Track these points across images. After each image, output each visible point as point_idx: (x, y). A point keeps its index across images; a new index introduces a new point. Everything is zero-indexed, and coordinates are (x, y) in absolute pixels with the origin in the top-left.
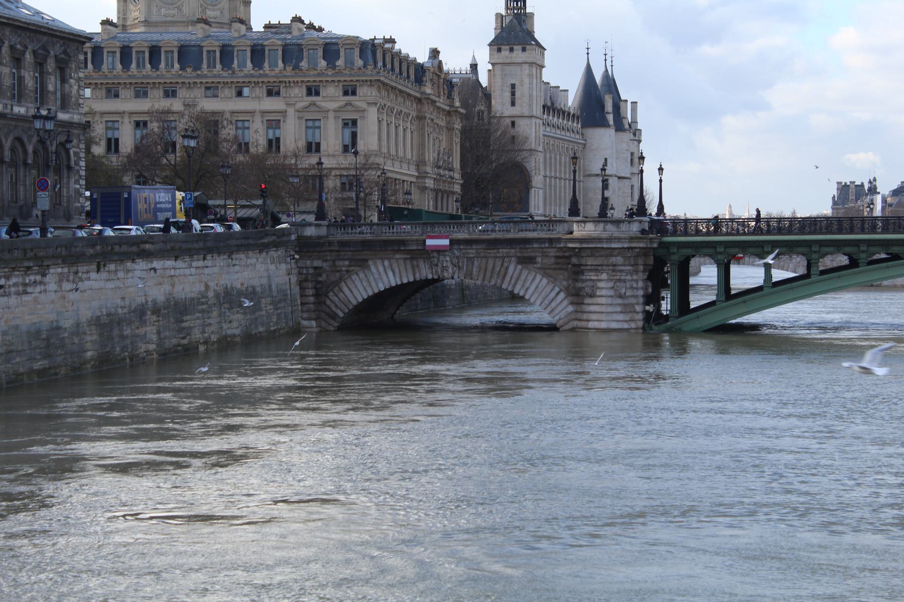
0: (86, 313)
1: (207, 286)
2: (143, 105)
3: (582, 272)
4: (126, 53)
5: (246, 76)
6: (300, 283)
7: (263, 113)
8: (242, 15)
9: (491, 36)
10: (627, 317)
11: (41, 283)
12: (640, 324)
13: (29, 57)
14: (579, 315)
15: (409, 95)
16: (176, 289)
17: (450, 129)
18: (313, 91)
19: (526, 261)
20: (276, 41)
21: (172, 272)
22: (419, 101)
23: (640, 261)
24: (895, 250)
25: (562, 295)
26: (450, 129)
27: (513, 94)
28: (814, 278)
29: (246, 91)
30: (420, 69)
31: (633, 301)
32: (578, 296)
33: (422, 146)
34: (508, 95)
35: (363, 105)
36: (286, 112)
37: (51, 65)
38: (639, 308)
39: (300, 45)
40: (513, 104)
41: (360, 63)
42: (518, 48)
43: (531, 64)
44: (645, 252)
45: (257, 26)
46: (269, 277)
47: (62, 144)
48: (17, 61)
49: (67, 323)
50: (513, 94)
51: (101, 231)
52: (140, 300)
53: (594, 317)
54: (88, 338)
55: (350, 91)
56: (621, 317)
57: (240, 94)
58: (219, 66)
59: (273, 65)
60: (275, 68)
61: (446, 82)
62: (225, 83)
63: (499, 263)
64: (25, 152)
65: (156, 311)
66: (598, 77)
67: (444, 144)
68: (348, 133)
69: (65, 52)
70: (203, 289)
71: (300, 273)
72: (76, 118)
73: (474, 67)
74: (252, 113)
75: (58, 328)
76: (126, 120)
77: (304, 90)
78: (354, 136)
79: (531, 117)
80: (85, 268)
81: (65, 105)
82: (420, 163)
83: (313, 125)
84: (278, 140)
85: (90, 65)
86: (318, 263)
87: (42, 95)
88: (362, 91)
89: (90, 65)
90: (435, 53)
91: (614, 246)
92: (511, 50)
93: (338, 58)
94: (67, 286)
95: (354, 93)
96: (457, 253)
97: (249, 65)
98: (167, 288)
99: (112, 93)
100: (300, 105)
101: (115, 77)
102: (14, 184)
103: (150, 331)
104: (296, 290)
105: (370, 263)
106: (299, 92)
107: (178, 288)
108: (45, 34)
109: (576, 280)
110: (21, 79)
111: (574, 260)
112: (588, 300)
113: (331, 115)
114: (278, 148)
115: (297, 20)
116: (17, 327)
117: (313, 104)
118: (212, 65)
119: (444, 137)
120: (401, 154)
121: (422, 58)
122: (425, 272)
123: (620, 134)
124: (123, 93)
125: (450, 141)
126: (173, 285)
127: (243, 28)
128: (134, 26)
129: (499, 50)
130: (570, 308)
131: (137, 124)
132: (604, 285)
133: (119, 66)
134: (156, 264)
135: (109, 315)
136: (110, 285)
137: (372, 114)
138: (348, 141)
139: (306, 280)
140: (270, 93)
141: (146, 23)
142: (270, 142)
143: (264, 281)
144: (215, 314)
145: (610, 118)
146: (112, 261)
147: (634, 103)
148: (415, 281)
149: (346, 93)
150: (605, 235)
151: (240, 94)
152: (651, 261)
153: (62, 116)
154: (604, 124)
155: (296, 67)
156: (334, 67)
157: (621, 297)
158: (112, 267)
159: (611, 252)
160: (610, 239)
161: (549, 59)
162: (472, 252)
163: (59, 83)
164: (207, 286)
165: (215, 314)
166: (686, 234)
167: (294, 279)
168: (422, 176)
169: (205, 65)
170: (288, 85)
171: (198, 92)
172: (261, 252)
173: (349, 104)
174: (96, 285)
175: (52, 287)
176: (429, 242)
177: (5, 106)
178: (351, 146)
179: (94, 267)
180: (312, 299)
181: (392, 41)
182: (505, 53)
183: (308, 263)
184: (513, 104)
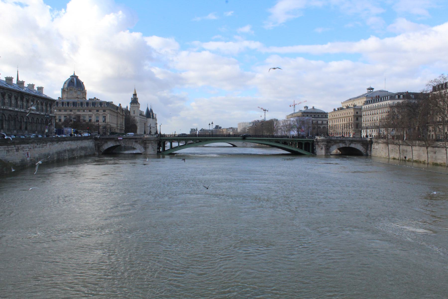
1: (77, 146)
2: (66, 113)
3: (146, 144)
4: (63, 103)
5: (85, 108)
6: (95, 146)
7: (88, 115)
8: (84, 97)
9: (130, 102)
10: (154, 152)
11: (46, 145)
12: (156, 153)
13: (44, 104)
14: (146, 151)
15: (115, 112)
16: (72, 147)
17: (123, 118)
18: (98, 111)
19: (136, 142)
20: (91, 102)
21: (71, 144)
22: (117, 113)
23: (157, 142)
24: (201, 140)
25: (143, 148)
26: (123, 118)
27: (134, 112)
28: (187, 145)
29: (85, 111)
30: (117, 107)
31: (155, 149)
32: (145, 148)
33: (118, 121)
34: (133, 112)
35: (107, 114)
36: (92, 115)
37: (48, 105)
38: (156, 150)
39: (95, 103)
40: (134, 114)
41: (106, 106)
42: (135, 104)
43: (137, 107)
44: (157, 140)
45: (87, 99)
46: (89, 145)
47: (50, 120)
48: (42, 104)
49: (51, 153)
50: (134, 112)
51: (58, 136)
52: (65, 149)
53: (148, 152)
54: (55, 156)
55: (104, 111)
56: (153, 152)
57: (84, 111)
58: (80, 106)
59: (90, 106)
60: (91, 107)
61: (122, 110)
62: (81, 109)
63: (131, 142)
64: (43, 121)
65: (68, 151)
66: (149, 110)
67: (122, 121)
68: (104, 118)
69: (51, 103)
70: (77, 146)
71: (95, 144)
72: (53, 115)
73: (127, 107)
74: (86, 115)
75: (49, 154)
76: (63, 116)
77: (96, 111)
78: (105, 119)
79: (137, 116)
80: (54, 143)
81: (51, 113)
82: (117, 124)
83: (97, 117)
84: (91, 120)
85: (56, 106)
86: (98, 142)
87: (47, 111)
89: (56, 106)
90: (120, 104)
91: (152, 139)
92: (134, 104)
93: (102, 105)
94: (51, 146)
95: (105, 111)
96: (124, 140)
97: (86, 106)
99: (60, 110)
100: (95, 113)
101: (61, 108)
102: (41, 127)
103: (67, 154)
104: (94, 147)
105: (108, 142)
106: (95, 111)
107: (72, 147)
108: (47, 100)
109: (145, 145)
110: (43, 108)
111: (145, 142)
112: (147, 149)
113: (101, 115)
114: (91, 121)
115: (95, 98)
116: (41, 154)
117: (98, 113)
118: (79, 106)
119: (122, 120)
120: (114, 122)
121: (118, 105)
122: (118, 144)
124: (62, 111)
125: (123, 120)
126: (71, 146)
127: (85, 99)
128: (64, 98)
129: (132, 104)
130: (144, 150)
131: (65, 116)
132: (150, 146)
133: (61, 106)
134: (68, 142)
135: (59, 151)
136: (59, 146)
137: (109, 115)
138: (104, 120)
139: (96, 145)
140: (90, 111)
141: (67, 98)
142: (90, 120)
143: (88, 145)
144: (79, 151)
145: (151, 117)
146: (60, 141)
147: (156, 114)
148: (116, 145)
149: (104, 111)
150: (150, 137)
151: (84, 111)
152: (158, 142)
153: (50, 115)
154: (150, 118)
155: (95, 106)
156: (102, 107)
157: (153, 148)
158: (60, 143)
159: (151, 140)
160: (151, 138)
161: (141, 106)
162: (126, 140)
164: (77, 146)
165: (79, 151)
166: (165, 137)
167: (94, 145)
168: (117, 126)
169: (78, 106)
170: (93, 110)
171: (76, 111)
172: (88, 140)
173: (104, 113)
174: (56, 146)
175: (48, 146)
176: (119, 138)
177: (40, 113)
178: (104, 121)
179: (56, 143)
180: (97, 149)
181: (112, 102)
183: (97, 142)
184: (134, 114)
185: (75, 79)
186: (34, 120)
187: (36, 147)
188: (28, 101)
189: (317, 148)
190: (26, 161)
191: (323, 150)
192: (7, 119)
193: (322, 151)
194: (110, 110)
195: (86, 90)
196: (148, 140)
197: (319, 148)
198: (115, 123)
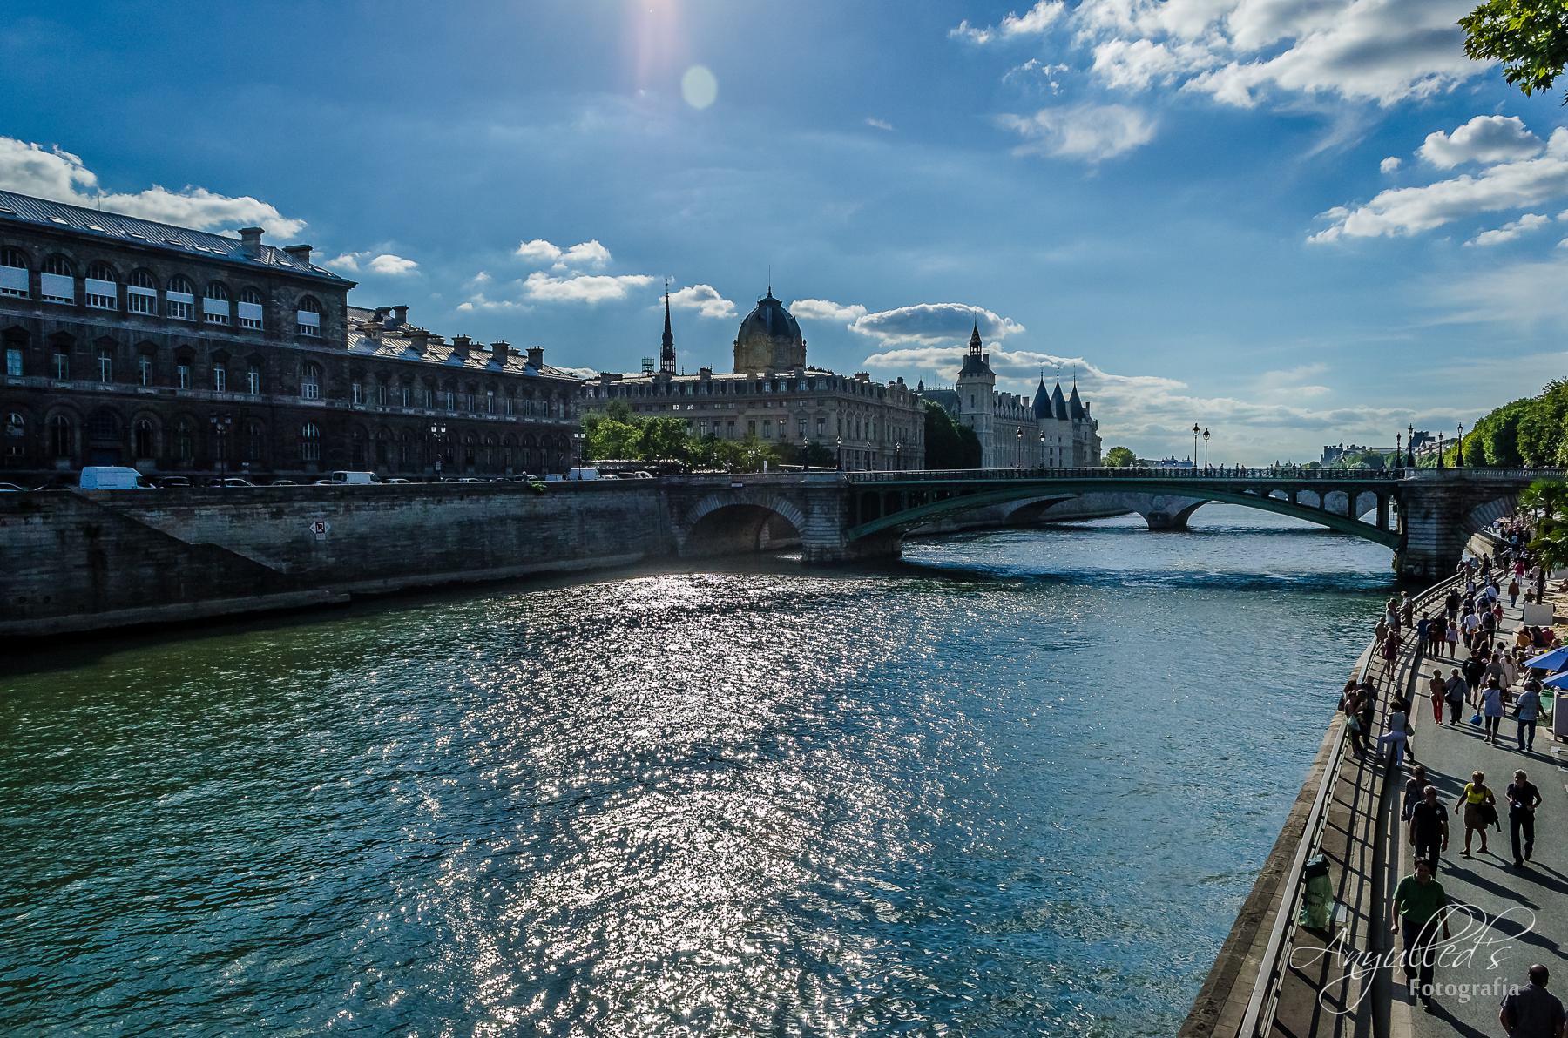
0: (447, 519)
1: (569, 508)
16: (537, 509)
19: (782, 494)
22: (880, 407)
27: (973, 401)
29: (769, 405)
32: (807, 513)
34: (969, 402)
37: (554, 397)
50: (973, 401)
55: (821, 402)
56: (826, 524)
57: (766, 406)
65: (517, 519)
88: (828, 403)
90: (900, 380)
98: (528, 508)
100: (796, 411)
107: (537, 509)
122: (733, 502)
123: (1064, 422)
129: (965, 376)
132: (817, 511)
137: (834, 416)
147: (1088, 404)
151: (766, 406)
153: (562, 422)
154: (1050, 416)
163: (561, 406)
181: (866, 376)
182: (968, 377)
185: (769, 310)
186: (518, 440)
187: (358, 508)
188: (472, 389)
189: (1409, 515)
190: (313, 542)
191: (1432, 521)
192: (396, 438)
193: (1426, 526)
194: (839, 401)
195: (805, 342)
196: (812, 490)
197: (1417, 515)
198: (871, 436)
